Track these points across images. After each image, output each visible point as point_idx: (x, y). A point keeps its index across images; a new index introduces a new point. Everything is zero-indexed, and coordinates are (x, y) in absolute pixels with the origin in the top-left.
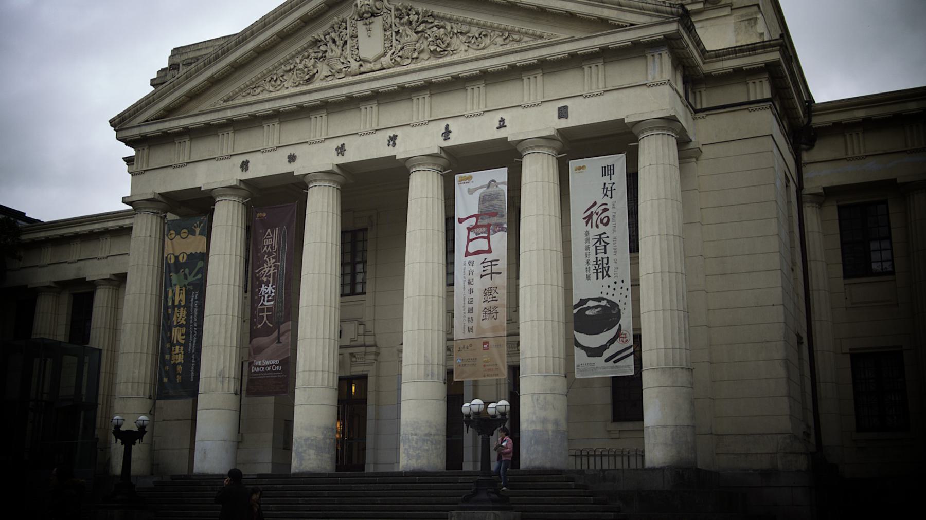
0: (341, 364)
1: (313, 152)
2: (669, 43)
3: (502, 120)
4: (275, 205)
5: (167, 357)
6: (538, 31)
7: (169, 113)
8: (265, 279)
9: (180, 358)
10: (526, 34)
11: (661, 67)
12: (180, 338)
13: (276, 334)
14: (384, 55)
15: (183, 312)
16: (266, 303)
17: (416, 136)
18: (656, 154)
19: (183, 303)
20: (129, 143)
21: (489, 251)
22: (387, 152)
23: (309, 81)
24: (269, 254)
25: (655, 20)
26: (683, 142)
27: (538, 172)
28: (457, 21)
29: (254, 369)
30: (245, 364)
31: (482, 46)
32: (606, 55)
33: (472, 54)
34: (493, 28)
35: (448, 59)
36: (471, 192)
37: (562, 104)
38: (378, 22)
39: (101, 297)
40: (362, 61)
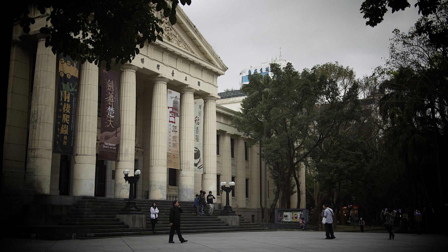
3: (186, 78)
5: (59, 129)
6: (194, 51)
8: (110, 104)
9: (66, 132)
10: (191, 49)
12: (66, 120)
13: (115, 132)
15: (68, 106)
16: (111, 116)
19: (68, 101)
21: (174, 123)
22: (156, 71)
24: (111, 92)
25: (221, 68)
28: (175, 31)
29: (104, 147)
30: (100, 144)
31: (180, 45)
33: (176, 46)
34: (183, 40)
35: (170, 43)
36: (172, 98)
37: (199, 81)
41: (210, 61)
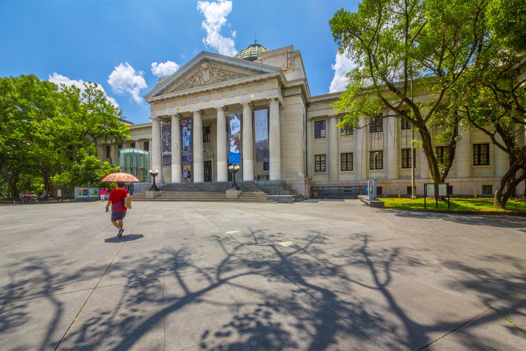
0: (204, 158)
1: (193, 107)
2: (278, 77)
4: (186, 120)
7: (157, 95)
11: (276, 84)
17: (217, 102)
18: (274, 108)
20: (149, 103)
23: (192, 87)
26: (280, 104)
27: (246, 112)
32: (262, 80)
38: (208, 70)
39: (150, 142)
40: (205, 82)
41: (262, 72)
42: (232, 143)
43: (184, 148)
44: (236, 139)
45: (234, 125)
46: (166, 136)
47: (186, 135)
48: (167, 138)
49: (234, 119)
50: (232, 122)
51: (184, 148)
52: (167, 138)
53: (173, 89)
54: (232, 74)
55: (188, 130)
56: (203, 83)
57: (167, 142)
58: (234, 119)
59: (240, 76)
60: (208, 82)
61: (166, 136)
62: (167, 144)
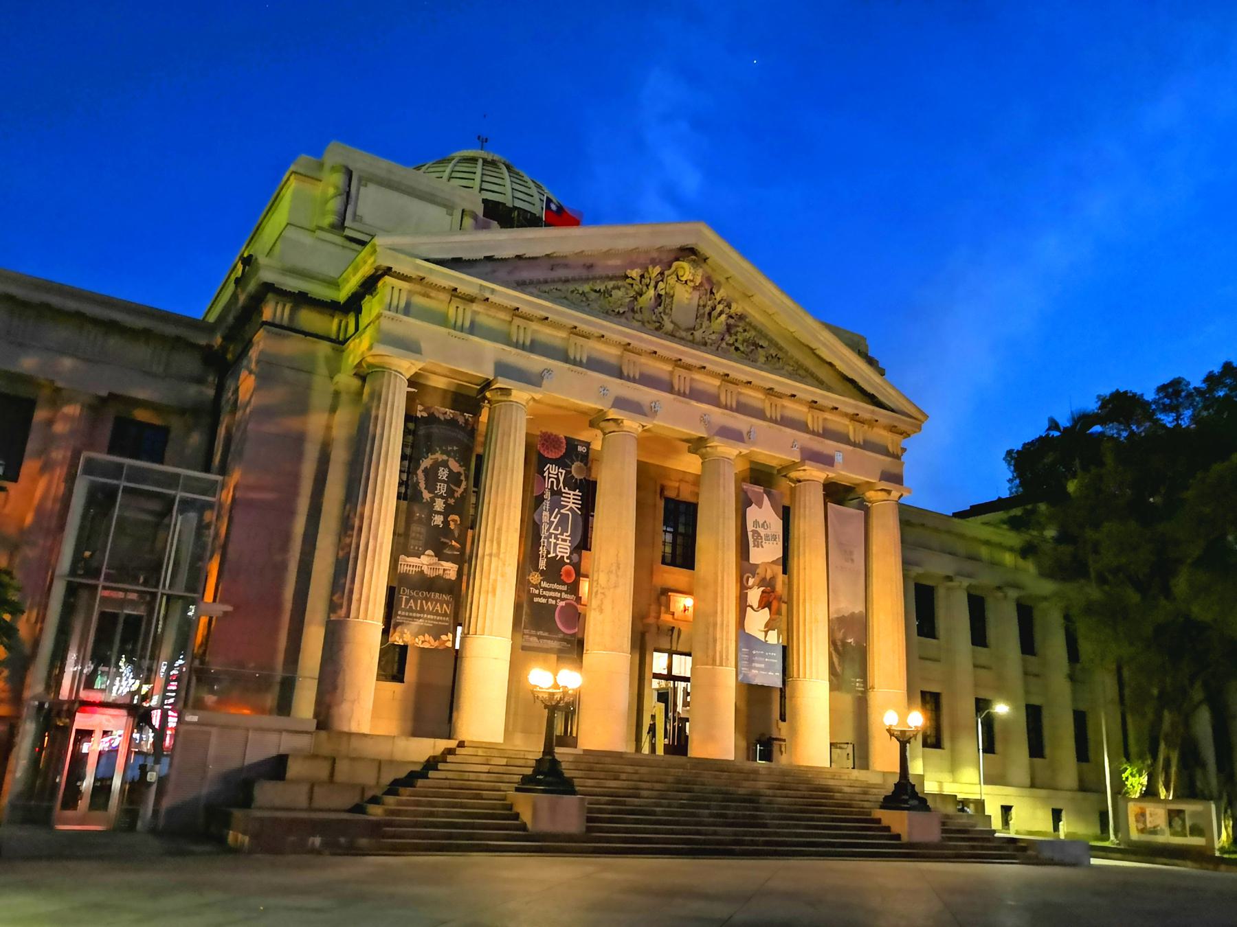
14: (694, 329)
42: (754, 596)
43: (542, 564)
44: (768, 586)
45: (762, 532)
46: (443, 474)
47: (556, 505)
48: (442, 488)
49: (760, 505)
50: (753, 513)
51: (542, 564)
52: (442, 488)
53: (525, 275)
54: (773, 352)
55: (571, 483)
56: (669, 326)
57: (439, 505)
58: (760, 505)
59: (820, 384)
60: (688, 330)
61: (443, 474)
62: (438, 520)
